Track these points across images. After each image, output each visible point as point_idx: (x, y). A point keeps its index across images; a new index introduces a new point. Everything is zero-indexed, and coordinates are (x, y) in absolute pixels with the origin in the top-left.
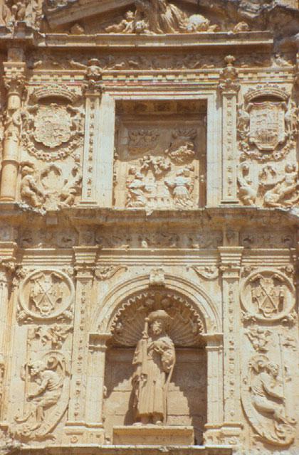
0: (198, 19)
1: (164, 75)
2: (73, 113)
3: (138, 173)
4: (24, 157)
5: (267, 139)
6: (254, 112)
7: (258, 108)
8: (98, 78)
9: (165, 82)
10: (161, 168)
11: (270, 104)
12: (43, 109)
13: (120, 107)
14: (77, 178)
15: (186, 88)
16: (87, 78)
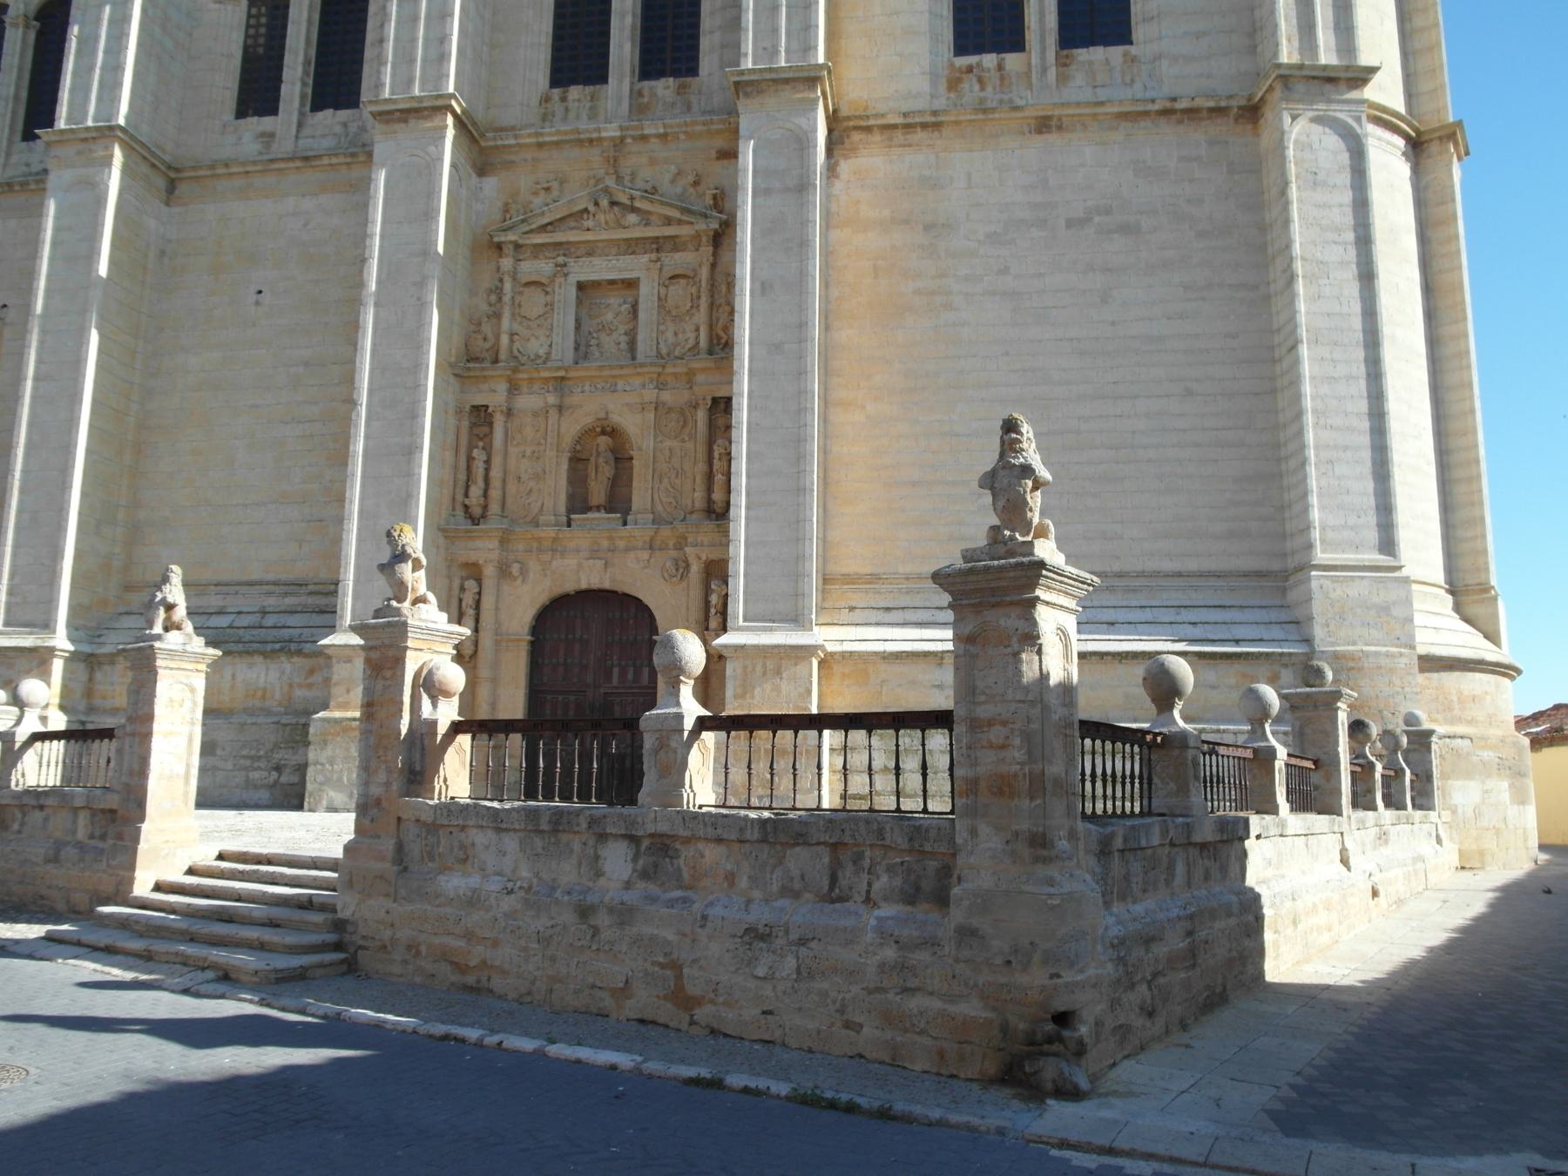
0: (632, 218)
1: (609, 260)
2: (547, 293)
3: (595, 335)
4: (516, 327)
5: (677, 307)
6: (671, 288)
7: (673, 284)
8: (565, 265)
9: (610, 265)
10: (610, 329)
11: (683, 281)
12: (526, 290)
13: (581, 286)
14: (549, 343)
15: (626, 270)
16: (557, 265)
